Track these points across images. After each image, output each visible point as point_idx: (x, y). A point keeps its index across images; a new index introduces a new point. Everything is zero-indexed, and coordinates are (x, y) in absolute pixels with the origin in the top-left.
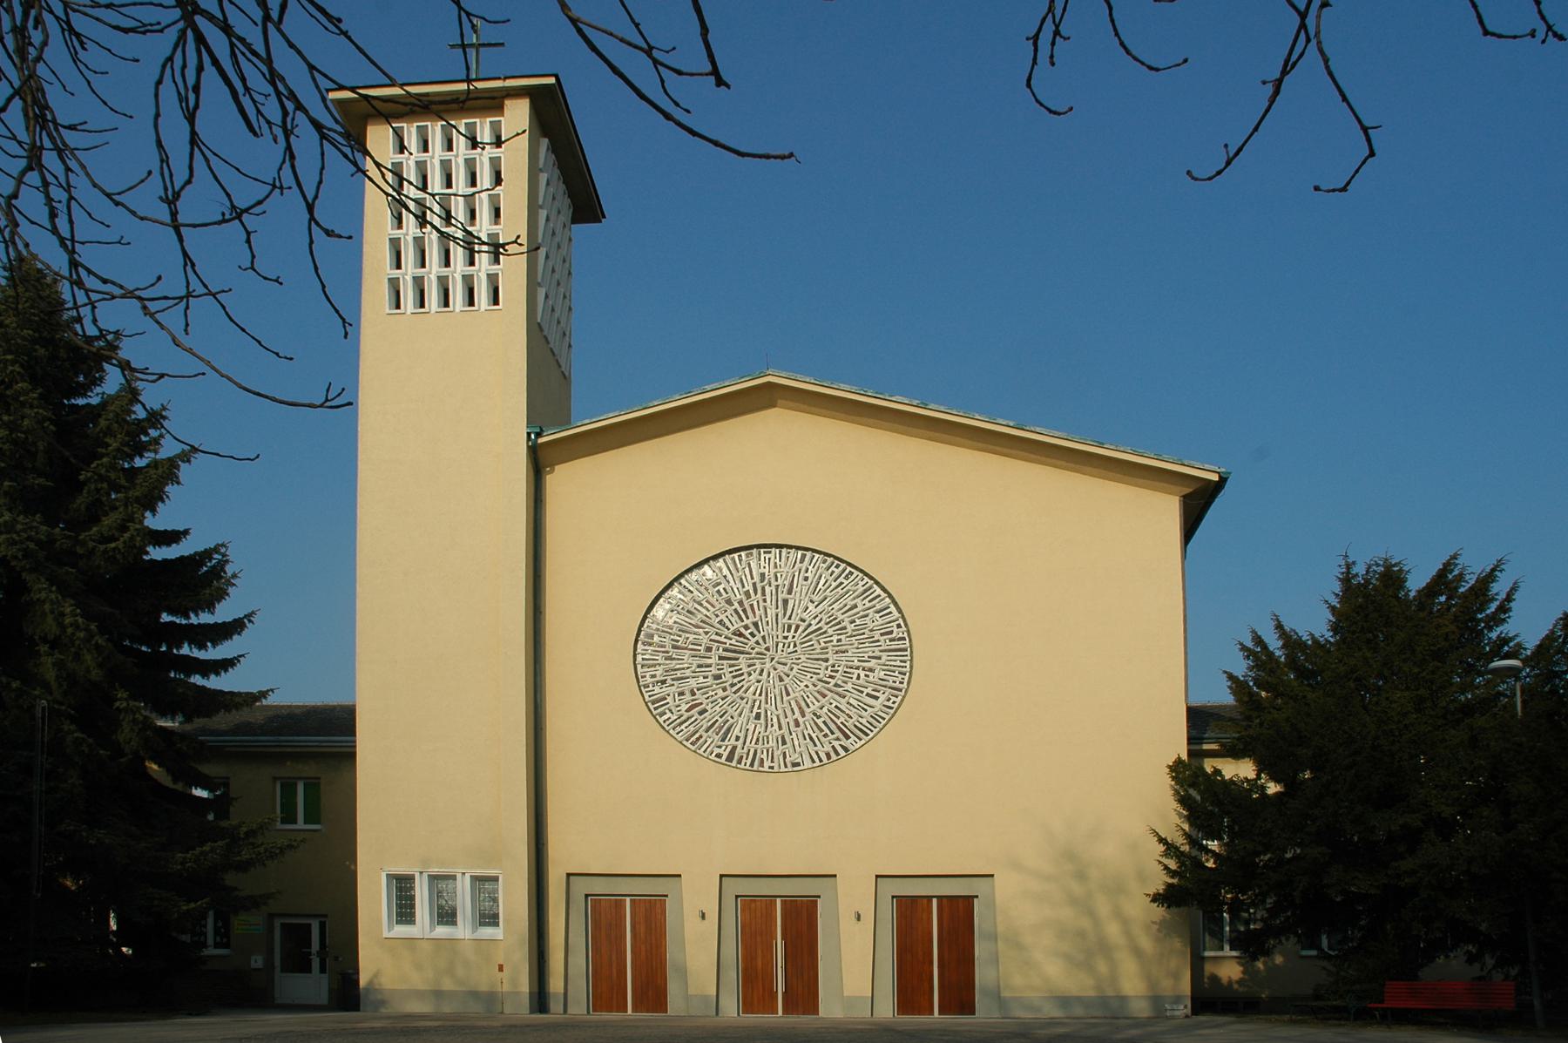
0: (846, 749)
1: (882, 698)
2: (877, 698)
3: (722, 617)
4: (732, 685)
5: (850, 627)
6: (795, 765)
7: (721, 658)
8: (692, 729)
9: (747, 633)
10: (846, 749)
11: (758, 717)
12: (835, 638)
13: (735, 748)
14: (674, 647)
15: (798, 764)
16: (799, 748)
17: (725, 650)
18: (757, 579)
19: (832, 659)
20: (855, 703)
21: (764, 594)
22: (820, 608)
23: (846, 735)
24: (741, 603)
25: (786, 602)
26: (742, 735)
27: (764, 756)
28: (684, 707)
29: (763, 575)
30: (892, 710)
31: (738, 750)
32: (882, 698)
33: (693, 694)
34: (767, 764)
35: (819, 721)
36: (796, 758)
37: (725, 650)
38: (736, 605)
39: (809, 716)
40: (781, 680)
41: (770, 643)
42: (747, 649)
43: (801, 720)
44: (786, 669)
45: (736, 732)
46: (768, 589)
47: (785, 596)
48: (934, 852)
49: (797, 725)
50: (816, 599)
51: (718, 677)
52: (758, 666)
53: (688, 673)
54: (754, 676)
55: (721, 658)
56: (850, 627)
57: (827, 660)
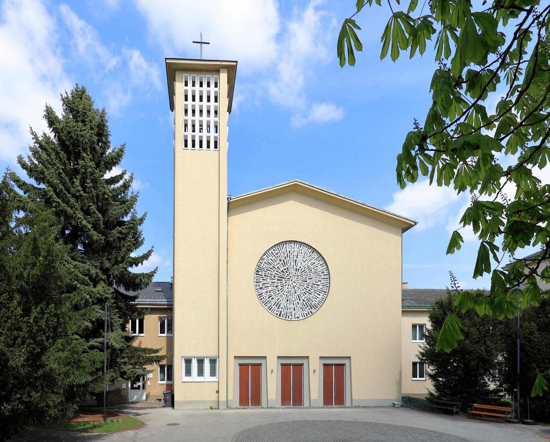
0: (311, 313)
1: (321, 295)
5: (313, 270)
6: (298, 318)
7: (278, 280)
8: (269, 305)
10: (311, 313)
11: (287, 301)
13: (281, 311)
14: (265, 276)
15: (298, 318)
16: (299, 313)
17: (279, 277)
18: (288, 252)
19: (308, 280)
23: (311, 308)
24: (283, 261)
25: (296, 261)
28: (267, 297)
29: (290, 251)
30: (324, 300)
32: (321, 295)
34: (290, 317)
36: (297, 315)
37: (279, 277)
39: (302, 301)
42: (285, 277)
44: (295, 284)
48: (335, 350)
50: (304, 260)
51: (277, 287)
53: (269, 285)
54: (287, 286)
55: (278, 280)
56: (313, 270)
57: (306, 281)
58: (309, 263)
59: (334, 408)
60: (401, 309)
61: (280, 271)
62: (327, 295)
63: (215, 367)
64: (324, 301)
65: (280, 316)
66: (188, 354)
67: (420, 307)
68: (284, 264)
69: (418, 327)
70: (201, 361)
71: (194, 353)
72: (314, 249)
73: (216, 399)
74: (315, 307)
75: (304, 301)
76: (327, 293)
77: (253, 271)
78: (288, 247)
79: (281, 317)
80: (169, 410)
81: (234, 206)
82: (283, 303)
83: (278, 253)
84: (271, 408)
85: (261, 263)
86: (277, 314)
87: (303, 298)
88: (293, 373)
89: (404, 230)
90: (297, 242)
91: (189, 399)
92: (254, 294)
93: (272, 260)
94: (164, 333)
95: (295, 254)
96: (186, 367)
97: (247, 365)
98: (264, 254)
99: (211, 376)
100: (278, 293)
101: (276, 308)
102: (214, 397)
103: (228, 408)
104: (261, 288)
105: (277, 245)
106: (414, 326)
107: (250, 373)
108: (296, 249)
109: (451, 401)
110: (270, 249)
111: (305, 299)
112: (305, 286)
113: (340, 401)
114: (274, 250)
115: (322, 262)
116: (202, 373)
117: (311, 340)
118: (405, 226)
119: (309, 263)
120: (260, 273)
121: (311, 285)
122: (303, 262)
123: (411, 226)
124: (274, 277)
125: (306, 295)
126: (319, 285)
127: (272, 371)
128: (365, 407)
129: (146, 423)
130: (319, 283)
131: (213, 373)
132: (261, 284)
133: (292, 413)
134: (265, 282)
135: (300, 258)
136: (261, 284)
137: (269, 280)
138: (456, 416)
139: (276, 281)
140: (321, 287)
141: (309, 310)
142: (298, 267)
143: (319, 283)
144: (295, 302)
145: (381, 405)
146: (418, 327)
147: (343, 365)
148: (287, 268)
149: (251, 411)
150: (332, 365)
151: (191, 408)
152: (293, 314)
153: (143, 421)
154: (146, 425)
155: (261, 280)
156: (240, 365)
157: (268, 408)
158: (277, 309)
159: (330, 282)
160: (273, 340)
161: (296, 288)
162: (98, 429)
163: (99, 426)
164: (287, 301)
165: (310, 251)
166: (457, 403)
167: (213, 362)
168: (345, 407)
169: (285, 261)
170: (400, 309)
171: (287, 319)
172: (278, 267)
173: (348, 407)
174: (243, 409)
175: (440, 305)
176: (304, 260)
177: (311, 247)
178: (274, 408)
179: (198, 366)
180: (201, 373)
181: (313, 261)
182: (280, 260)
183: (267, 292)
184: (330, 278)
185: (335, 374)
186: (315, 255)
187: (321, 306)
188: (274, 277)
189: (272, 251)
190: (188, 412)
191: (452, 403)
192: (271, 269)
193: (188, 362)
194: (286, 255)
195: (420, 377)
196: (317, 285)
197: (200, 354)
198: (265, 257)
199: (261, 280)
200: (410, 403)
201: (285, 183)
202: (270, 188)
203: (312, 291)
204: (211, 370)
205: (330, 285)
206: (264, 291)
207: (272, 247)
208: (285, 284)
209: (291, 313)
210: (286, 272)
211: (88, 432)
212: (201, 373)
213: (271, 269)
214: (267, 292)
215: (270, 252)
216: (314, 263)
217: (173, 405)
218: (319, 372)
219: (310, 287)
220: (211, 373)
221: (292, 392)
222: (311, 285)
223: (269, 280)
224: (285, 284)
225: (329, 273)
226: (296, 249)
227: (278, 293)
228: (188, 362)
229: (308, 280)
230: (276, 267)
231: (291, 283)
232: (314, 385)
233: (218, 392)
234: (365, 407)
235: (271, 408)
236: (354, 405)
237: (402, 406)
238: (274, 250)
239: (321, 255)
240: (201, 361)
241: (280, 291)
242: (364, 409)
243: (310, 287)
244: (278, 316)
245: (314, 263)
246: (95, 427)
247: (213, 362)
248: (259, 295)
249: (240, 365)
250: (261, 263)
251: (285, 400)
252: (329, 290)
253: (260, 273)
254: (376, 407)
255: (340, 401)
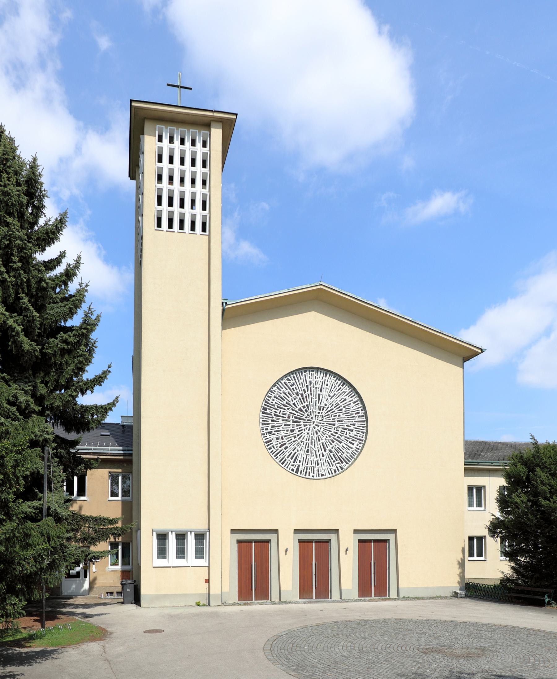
0: (342, 468)
1: (356, 444)
2: (353, 444)
3: (295, 401)
4: (298, 435)
5: (344, 409)
6: (323, 475)
7: (294, 422)
8: (282, 456)
9: (304, 410)
10: (342, 468)
11: (308, 451)
12: (338, 414)
13: (299, 466)
14: (275, 415)
15: (323, 475)
16: (324, 468)
17: (295, 418)
18: (308, 383)
19: (337, 423)
20: (345, 446)
21: (311, 392)
22: (332, 400)
23: (342, 461)
24: (302, 395)
25: (319, 395)
26: (302, 460)
27: (310, 471)
28: (279, 445)
29: (310, 382)
30: (359, 451)
31: (300, 467)
32: (356, 444)
33: (282, 439)
34: (312, 474)
35: (332, 454)
37: (295, 418)
38: (300, 396)
39: (328, 452)
40: (317, 433)
41: (313, 416)
42: (304, 418)
43: (324, 453)
44: (319, 428)
45: (299, 459)
46: (312, 389)
47: (318, 392)
49: (323, 456)
50: (332, 395)
51: (292, 431)
52: (308, 426)
53: (281, 428)
54: (307, 431)
57: (334, 425)
58: (339, 399)
59: (373, 600)
60: (463, 466)
61: (297, 409)
62: (364, 445)
63: (203, 544)
64: (360, 453)
65: (297, 472)
66: (162, 527)
67: (492, 464)
68: (303, 399)
69: (475, 490)
70: (181, 537)
71: (172, 524)
72: (345, 380)
73: (205, 592)
74: (347, 461)
75: (331, 452)
76: (363, 442)
77: (259, 409)
78: (309, 376)
79: (299, 474)
80: (132, 607)
81: (232, 316)
82: (302, 455)
83: (293, 385)
84: (285, 602)
85: (270, 397)
86: (293, 470)
87: (330, 448)
88: (315, 551)
89: (466, 359)
90: (321, 369)
91: (163, 592)
92: (260, 441)
93: (285, 394)
95: (319, 386)
96: (159, 544)
97: (310, 541)
98: (274, 385)
99: (196, 557)
100: (293, 439)
101: (292, 461)
102: (202, 588)
103: (225, 604)
104: (269, 433)
105: (292, 373)
106: (470, 489)
107: (254, 555)
108: (320, 379)
109: (538, 587)
110: (282, 378)
111: (333, 450)
112: (333, 431)
113: (382, 590)
114: (288, 380)
115: (357, 399)
116: (184, 553)
117: (342, 506)
118: (467, 354)
119: (339, 399)
120: (268, 411)
121: (340, 429)
122: (329, 398)
123: (477, 354)
124: (289, 417)
125: (333, 444)
126: (351, 430)
127: (286, 550)
128: (416, 598)
129: (109, 629)
130: (352, 427)
131: (200, 554)
132: (269, 427)
133: (315, 608)
134: (275, 424)
135: (325, 392)
136: (269, 427)
137: (281, 422)
138: (548, 608)
139: (291, 423)
140: (354, 433)
141: (338, 465)
142: (323, 405)
143: (352, 427)
144: (318, 454)
145: (438, 595)
146: (475, 490)
147: (386, 541)
148: (307, 405)
149: (257, 607)
150: (370, 541)
151: (167, 604)
152: (316, 469)
153: (103, 626)
154: (111, 633)
155: (270, 422)
156: (239, 542)
157: (280, 602)
158: (292, 463)
159: (367, 427)
160: (288, 506)
161: (319, 434)
162: (37, 642)
163: (39, 637)
164: (308, 451)
165: (339, 382)
166: (549, 590)
167: (200, 537)
168: (390, 599)
169: (304, 395)
170: (462, 467)
171: (307, 476)
172: (294, 404)
173: (394, 599)
174: (245, 604)
175: (521, 460)
176: (332, 395)
177: (339, 377)
178: (290, 602)
179: (178, 544)
180: (181, 553)
181: (343, 397)
182: (297, 394)
183: (278, 439)
184: (367, 420)
185: (376, 552)
186: (346, 389)
187: (355, 460)
188: (289, 417)
189: (285, 380)
190: (166, 611)
191: (540, 590)
192: (284, 405)
193: (162, 537)
194: (305, 388)
195: (477, 556)
196: (349, 430)
197: (181, 527)
198: (275, 388)
199: (270, 422)
200: (473, 591)
201: (305, 287)
202: (283, 292)
203: (343, 438)
204: (196, 549)
205: (367, 430)
206: (274, 436)
207: (285, 376)
208: (303, 428)
209: (313, 468)
210: (306, 411)
211: (23, 647)
212: (181, 553)
213: (284, 405)
214: (278, 439)
215: (283, 382)
216: (345, 400)
217: (137, 600)
218: (354, 551)
219: (339, 432)
220: (196, 553)
221: (315, 578)
222: (340, 429)
223: (281, 422)
224: (303, 428)
225: (366, 413)
226: (320, 379)
227: (293, 439)
228: (162, 537)
229: (337, 423)
230: (291, 403)
231: (312, 426)
232: (346, 569)
233: (208, 581)
234: (416, 598)
235: (285, 602)
236: (401, 596)
237: (466, 596)
238: (288, 380)
239: (354, 389)
240: (181, 537)
241: (298, 437)
242: (417, 602)
243: (339, 432)
244: (294, 472)
245: (345, 400)
246: (31, 638)
247: (200, 537)
248: (267, 442)
249: (239, 542)
250: (270, 397)
251: (305, 590)
252: (366, 438)
253: (268, 411)
254: (433, 598)
255: (382, 590)
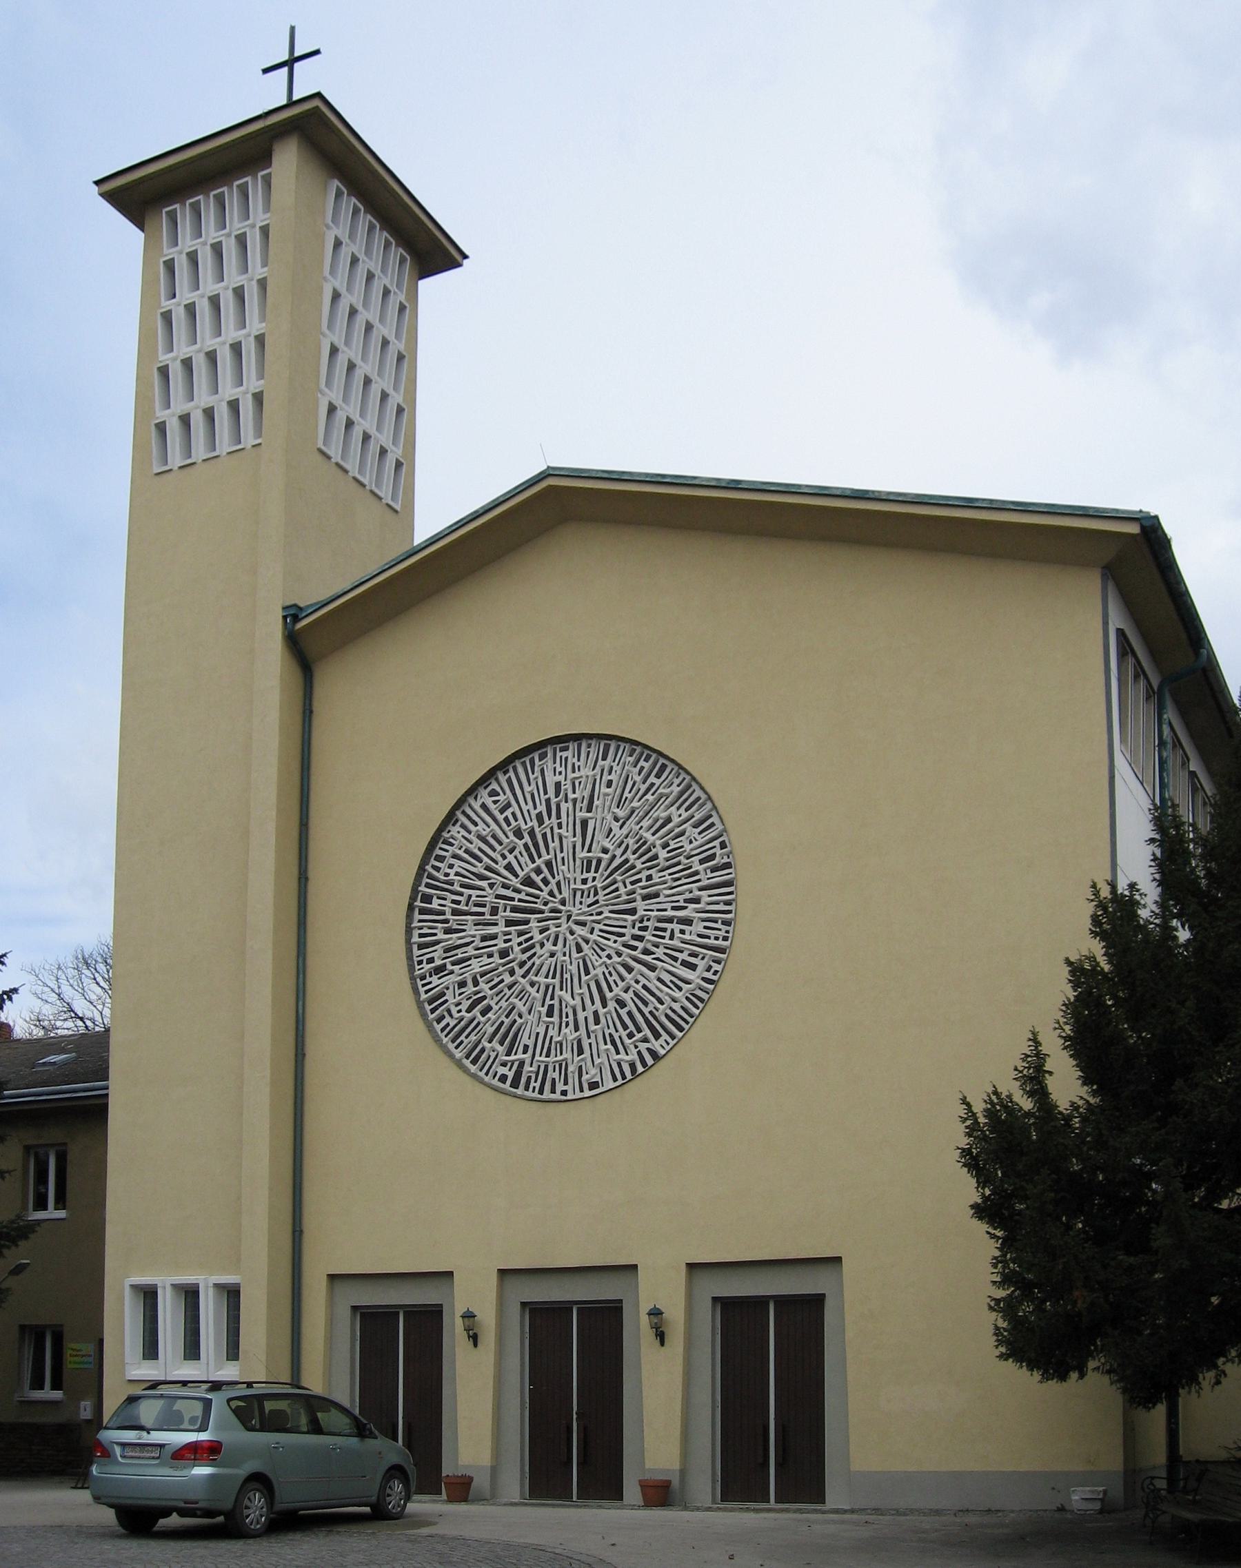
2: (693, 967)
3: (510, 858)
4: (522, 964)
5: (663, 854)
6: (593, 1085)
7: (509, 923)
8: (473, 1038)
9: (538, 879)
12: (643, 875)
13: (522, 1064)
14: (455, 912)
17: (515, 909)
19: (641, 905)
20: (667, 978)
21: (559, 817)
22: (625, 831)
25: (584, 823)
26: (531, 1043)
27: (556, 1075)
28: (466, 1005)
29: (558, 785)
31: (527, 1068)
33: (476, 983)
34: (560, 1087)
35: (623, 1012)
36: (591, 1074)
37: (515, 909)
38: (527, 838)
39: (612, 1005)
40: (579, 950)
41: (566, 893)
43: (602, 1011)
45: (525, 1040)
46: (564, 806)
47: (582, 815)
48: (760, 1226)
49: (597, 1022)
50: (621, 813)
51: (504, 954)
52: (553, 930)
53: (470, 951)
54: (549, 946)
55: (509, 923)
56: (663, 854)
57: (633, 912)
61: (515, 882)
65: (515, 1084)
75: (622, 1004)
78: (551, 770)
82: (532, 1026)
83: (508, 805)
85: (440, 859)
86: (503, 1078)
88: (575, 1348)
93: (483, 839)
94: (45, 1208)
95: (582, 793)
100: (508, 980)
104: (440, 970)
108: (586, 772)
110: (472, 791)
111: (627, 997)
112: (628, 932)
119: (646, 823)
120: (435, 904)
122: (615, 826)
126: (688, 921)
132: (438, 953)
136: (438, 953)
137: (471, 930)
139: (500, 929)
140: (699, 927)
141: (643, 1047)
142: (596, 853)
144: (581, 1016)
148: (549, 864)
155: (441, 936)
164: (550, 1013)
171: (547, 1094)
172: (509, 867)
176: (621, 813)
182: (518, 834)
183: (462, 984)
189: (484, 796)
194: (542, 808)
199: (441, 936)
203: (660, 952)
207: (483, 781)
209: (563, 1066)
214: (462, 984)
216: (669, 820)
223: (471, 930)
227: (508, 980)
232: (667, 1403)
243: (648, 935)
245: (669, 820)
250: (440, 859)
253: (435, 904)
